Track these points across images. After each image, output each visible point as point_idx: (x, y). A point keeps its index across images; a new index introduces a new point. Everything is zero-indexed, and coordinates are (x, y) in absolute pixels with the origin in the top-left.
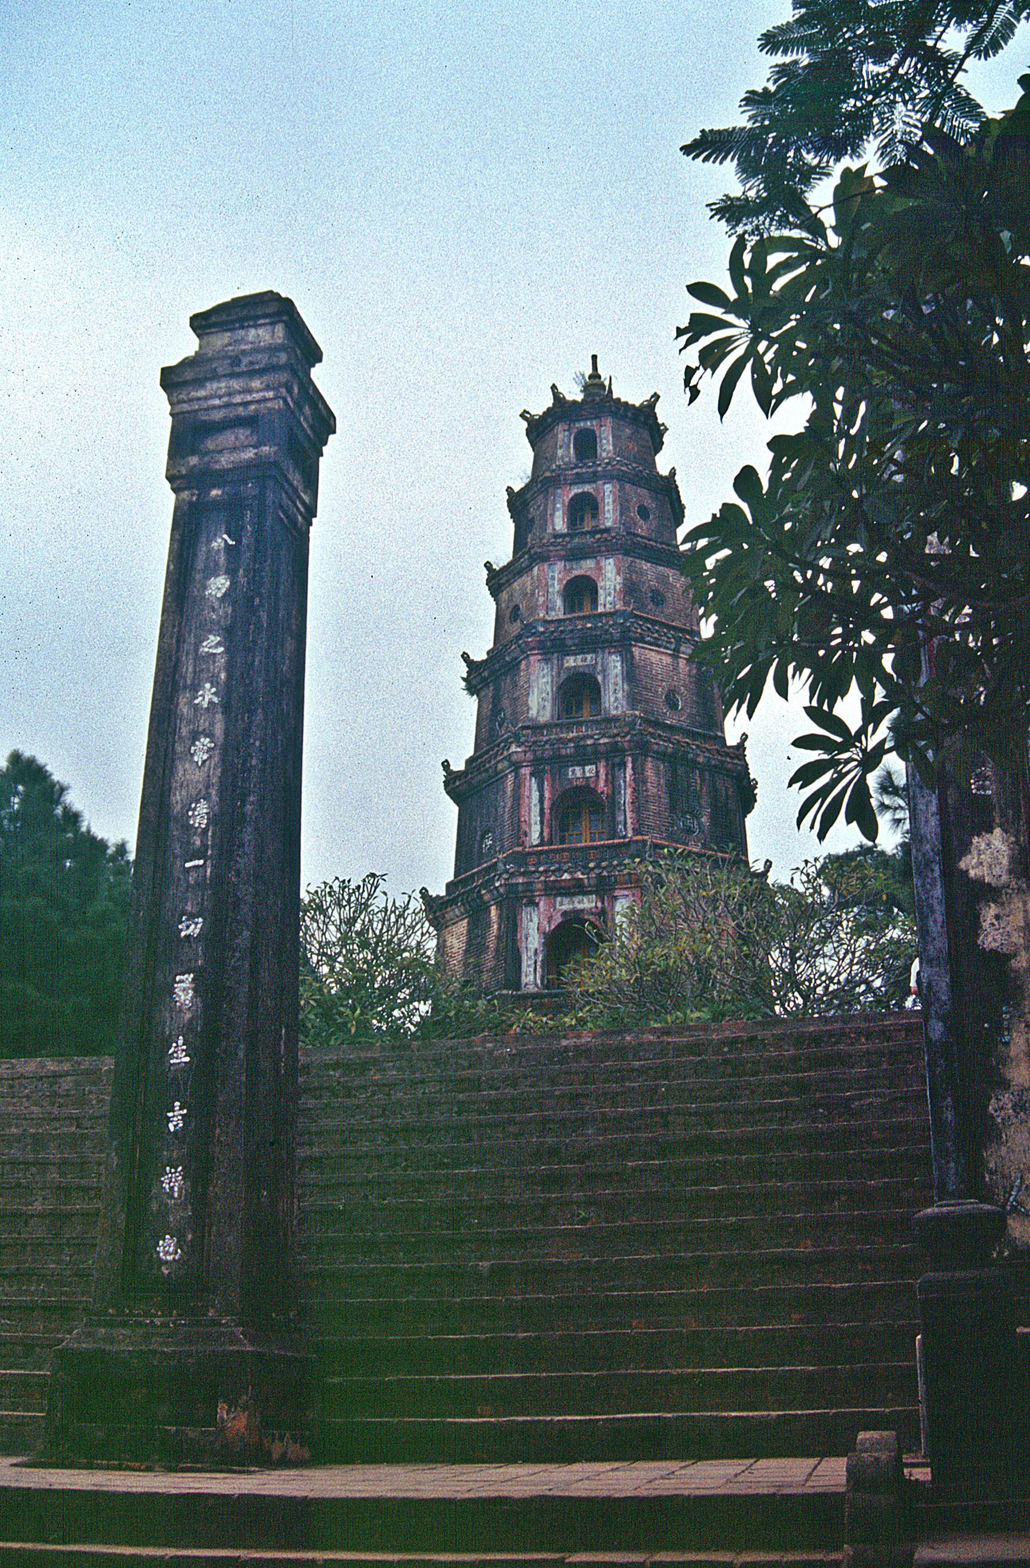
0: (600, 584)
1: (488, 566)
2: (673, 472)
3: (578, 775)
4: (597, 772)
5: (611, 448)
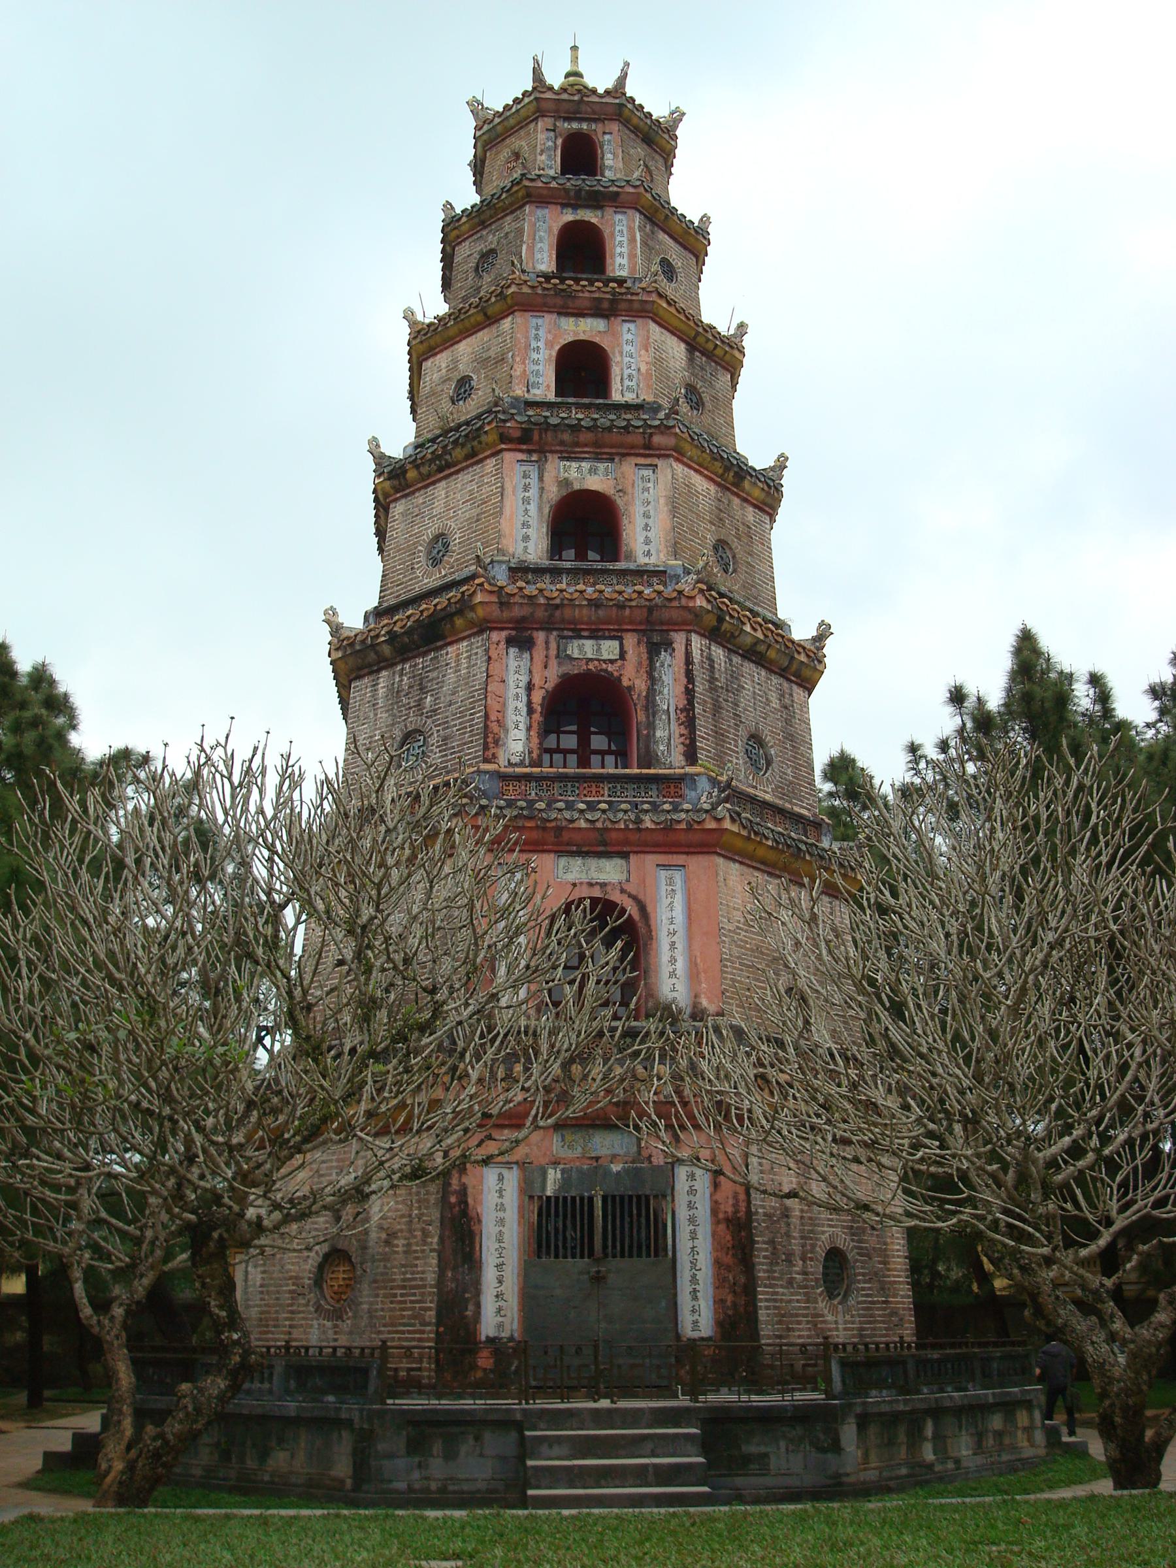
1: (409, 315)
2: (705, 220)
4: (623, 655)
5: (621, 165)
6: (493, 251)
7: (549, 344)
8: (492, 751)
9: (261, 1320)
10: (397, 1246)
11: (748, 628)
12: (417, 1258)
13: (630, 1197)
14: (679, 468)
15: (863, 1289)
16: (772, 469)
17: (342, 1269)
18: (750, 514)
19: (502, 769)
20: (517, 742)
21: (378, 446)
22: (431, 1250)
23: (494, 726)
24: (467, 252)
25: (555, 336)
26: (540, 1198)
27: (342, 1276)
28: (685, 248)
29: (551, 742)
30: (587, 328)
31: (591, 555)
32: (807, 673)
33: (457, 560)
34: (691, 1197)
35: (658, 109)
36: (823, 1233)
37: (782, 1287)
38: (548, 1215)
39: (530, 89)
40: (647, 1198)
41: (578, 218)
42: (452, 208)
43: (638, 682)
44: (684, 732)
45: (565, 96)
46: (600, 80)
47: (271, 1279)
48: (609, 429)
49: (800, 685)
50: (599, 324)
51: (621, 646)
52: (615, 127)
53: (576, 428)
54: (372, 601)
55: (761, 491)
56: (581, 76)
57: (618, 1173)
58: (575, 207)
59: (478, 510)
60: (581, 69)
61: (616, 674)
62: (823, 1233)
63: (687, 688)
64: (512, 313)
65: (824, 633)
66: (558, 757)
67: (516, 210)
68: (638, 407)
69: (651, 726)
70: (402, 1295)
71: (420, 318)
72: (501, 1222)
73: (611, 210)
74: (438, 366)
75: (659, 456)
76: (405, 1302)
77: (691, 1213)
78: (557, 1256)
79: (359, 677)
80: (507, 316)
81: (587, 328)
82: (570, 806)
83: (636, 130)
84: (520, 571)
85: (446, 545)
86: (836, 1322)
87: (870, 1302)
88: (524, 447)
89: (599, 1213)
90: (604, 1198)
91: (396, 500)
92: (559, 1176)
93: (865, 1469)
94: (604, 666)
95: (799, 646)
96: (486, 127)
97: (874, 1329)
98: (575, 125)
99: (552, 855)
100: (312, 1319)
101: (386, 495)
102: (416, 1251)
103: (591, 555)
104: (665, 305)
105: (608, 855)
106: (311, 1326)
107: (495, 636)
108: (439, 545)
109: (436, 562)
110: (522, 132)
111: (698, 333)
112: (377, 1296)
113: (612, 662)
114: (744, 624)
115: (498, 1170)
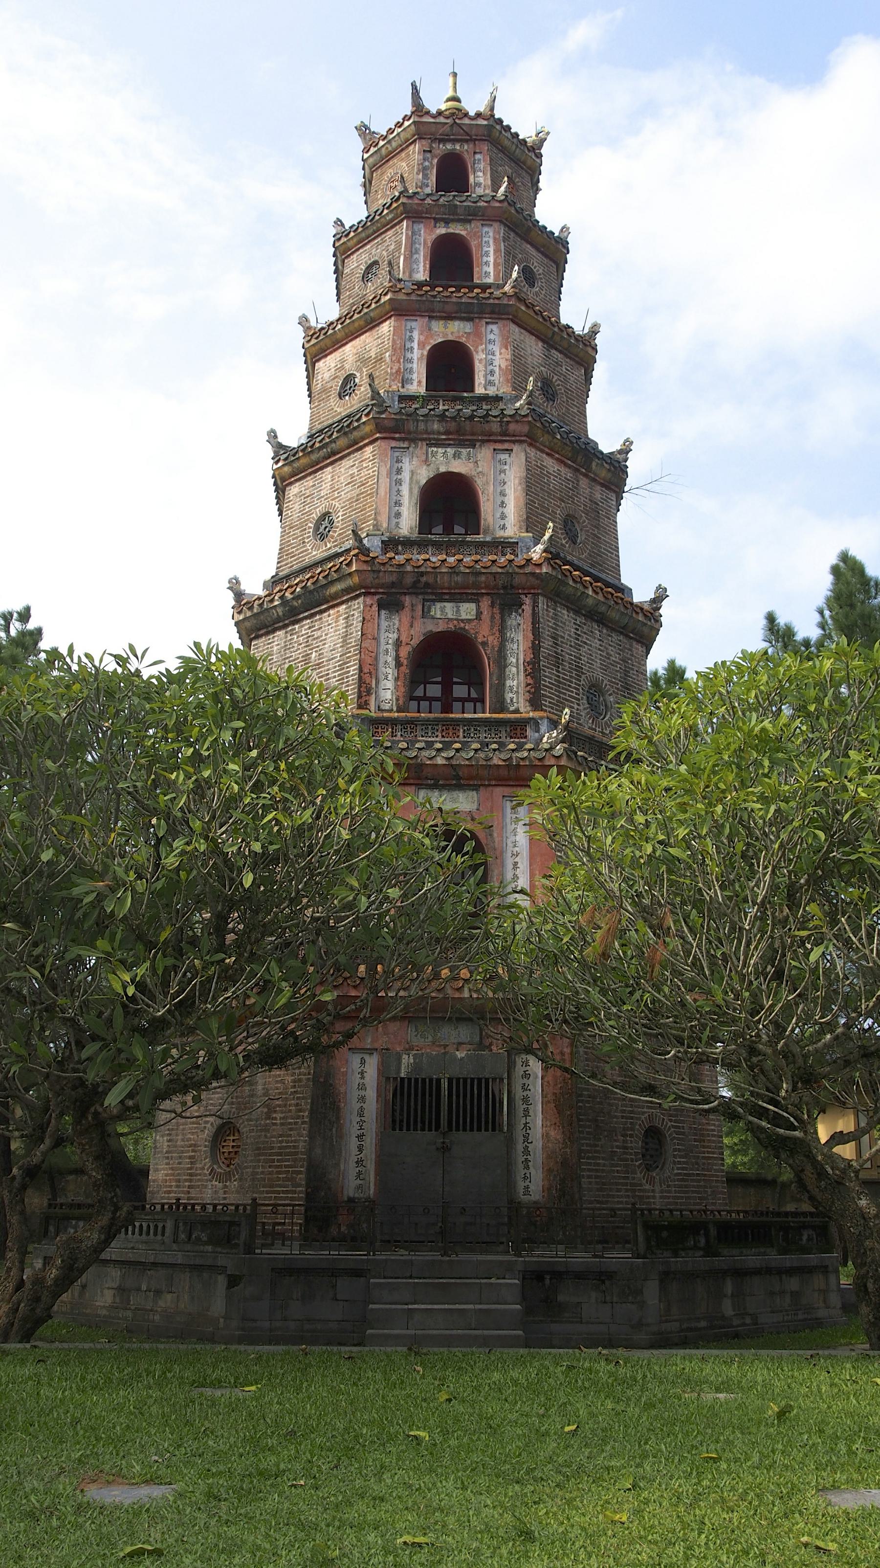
0: (479, 357)
1: (303, 321)
3: (450, 616)
4: (479, 614)
6: (376, 263)
7: (421, 345)
8: (364, 699)
9: (166, 1181)
10: (276, 1119)
11: (590, 592)
12: (291, 1129)
13: (472, 1080)
14: (532, 452)
15: (679, 1163)
16: (620, 452)
17: (232, 1138)
18: (598, 493)
19: (373, 714)
20: (388, 692)
21: (276, 437)
22: (303, 1123)
23: (367, 678)
24: (357, 263)
25: (427, 337)
26: (395, 1079)
27: (232, 1144)
28: (546, 256)
29: (419, 692)
30: (455, 330)
31: (458, 529)
32: (646, 630)
33: (340, 534)
34: (525, 1081)
35: (526, 131)
36: (643, 1113)
37: (603, 1159)
38: (402, 1094)
39: (409, 113)
40: (487, 1080)
41: (451, 231)
42: (343, 225)
43: (490, 639)
44: (530, 681)
45: (442, 120)
46: (473, 104)
47: (175, 1146)
48: (471, 418)
49: (638, 642)
50: (468, 327)
51: (478, 608)
52: (485, 147)
53: (442, 417)
54: (270, 571)
55: (610, 473)
56: (458, 100)
57: (462, 1059)
58: (447, 222)
59: (358, 491)
60: (459, 94)
61: (472, 631)
62: (643, 1113)
63: (533, 643)
64: (390, 318)
65: (661, 596)
66: (424, 704)
67: (395, 225)
68: (498, 399)
69: (502, 677)
70: (278, 1161)
71: (313, 323)
72: (362, 1099)
73: (479, 224)
74: (327, 366)
75: (514, 442)
76: (281, 1166)
77: (525, 1093)
78: (408, 1129)
79: (257, 637)
80: (385, 320)
81: (455, 330)
82: (429, 745)
83: (503, 150)
84: (392, 544)
85: (331, 522)
86: (653, 1191)
87: (685, 1174)
88: (397, 436)
89: (445, 1092)
90: (450, 1080)
91: (291, 484)
92: (412, 1061)
93: (666, 1321)
94: (462, 625)
95: (638, 608)
96: (373, 150)
97: (689, 1198)
98: (449, 146)
99: (413, 788)
100: (207, 1181)
101: (283, 479)
102: (290, 1123)
103: (458, 529)
104: (523, 308)
105: (460, 787)
106: (206, 1187)
107: (369, 600)
108: (323, 525)
109: (322, 537)
110: (403, 154)
111: (554, 333)
112: (259, 1161)
113: (469, 621)
114: (586, 588)
115: (361, 1056)
